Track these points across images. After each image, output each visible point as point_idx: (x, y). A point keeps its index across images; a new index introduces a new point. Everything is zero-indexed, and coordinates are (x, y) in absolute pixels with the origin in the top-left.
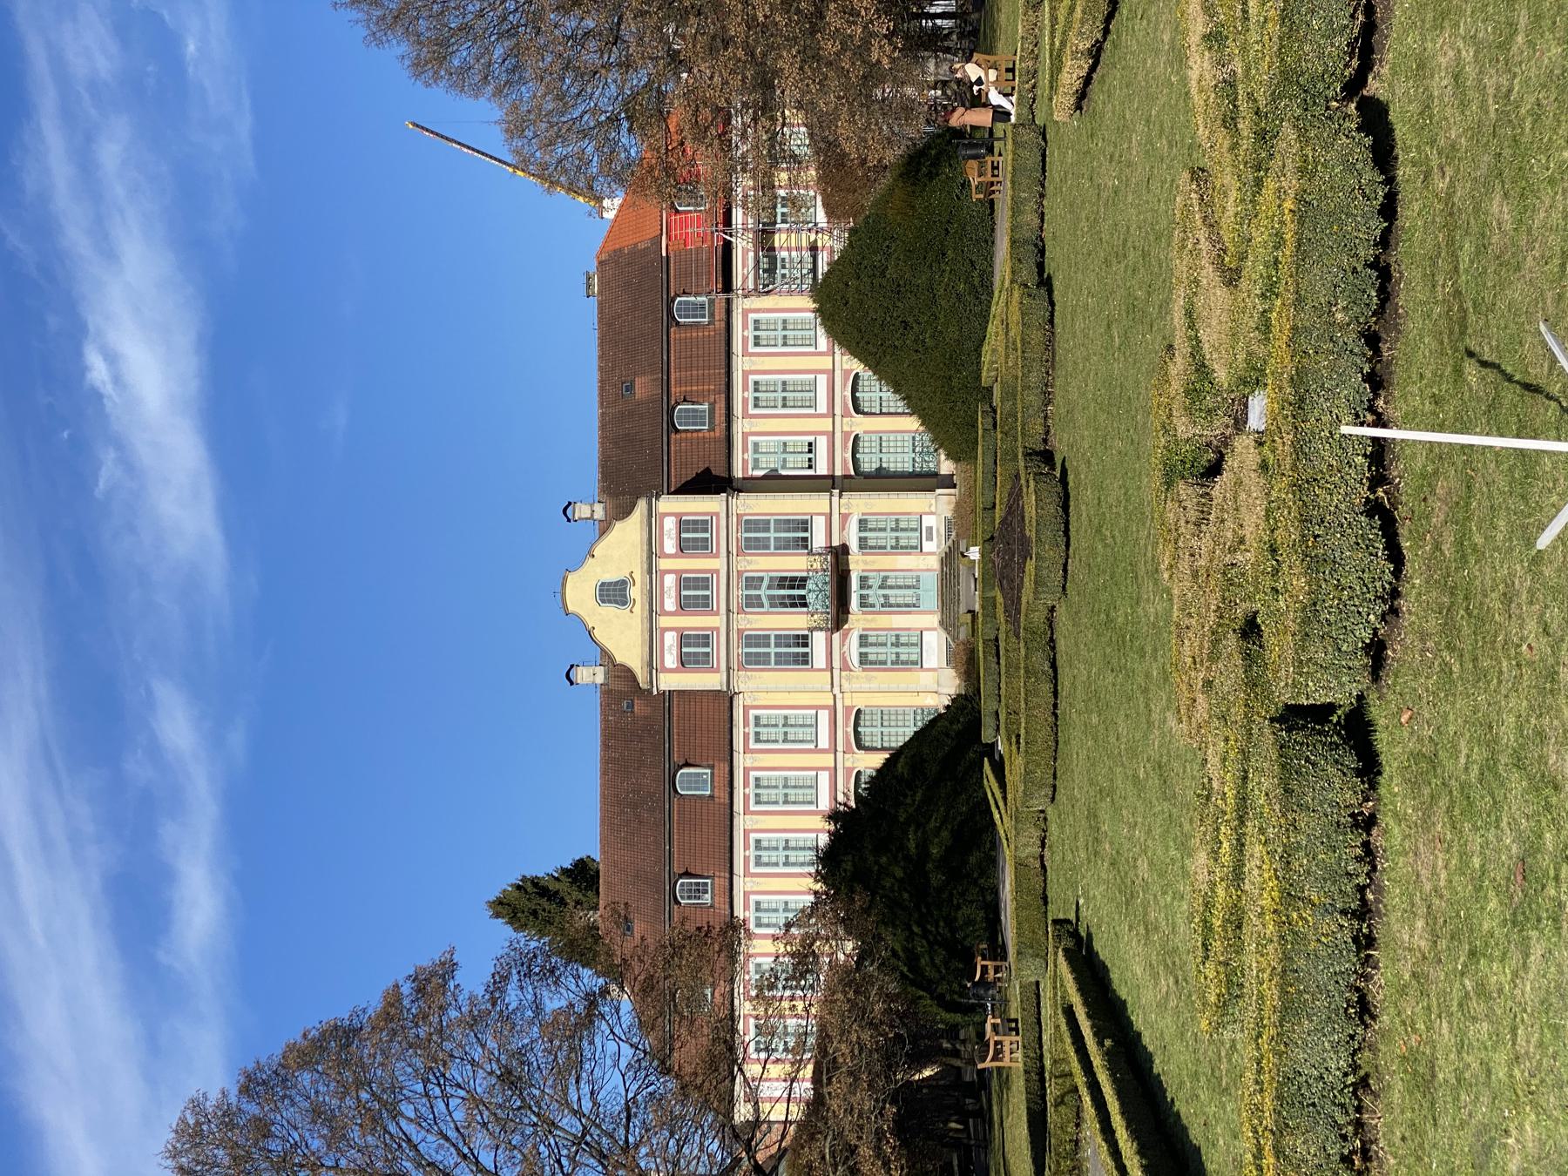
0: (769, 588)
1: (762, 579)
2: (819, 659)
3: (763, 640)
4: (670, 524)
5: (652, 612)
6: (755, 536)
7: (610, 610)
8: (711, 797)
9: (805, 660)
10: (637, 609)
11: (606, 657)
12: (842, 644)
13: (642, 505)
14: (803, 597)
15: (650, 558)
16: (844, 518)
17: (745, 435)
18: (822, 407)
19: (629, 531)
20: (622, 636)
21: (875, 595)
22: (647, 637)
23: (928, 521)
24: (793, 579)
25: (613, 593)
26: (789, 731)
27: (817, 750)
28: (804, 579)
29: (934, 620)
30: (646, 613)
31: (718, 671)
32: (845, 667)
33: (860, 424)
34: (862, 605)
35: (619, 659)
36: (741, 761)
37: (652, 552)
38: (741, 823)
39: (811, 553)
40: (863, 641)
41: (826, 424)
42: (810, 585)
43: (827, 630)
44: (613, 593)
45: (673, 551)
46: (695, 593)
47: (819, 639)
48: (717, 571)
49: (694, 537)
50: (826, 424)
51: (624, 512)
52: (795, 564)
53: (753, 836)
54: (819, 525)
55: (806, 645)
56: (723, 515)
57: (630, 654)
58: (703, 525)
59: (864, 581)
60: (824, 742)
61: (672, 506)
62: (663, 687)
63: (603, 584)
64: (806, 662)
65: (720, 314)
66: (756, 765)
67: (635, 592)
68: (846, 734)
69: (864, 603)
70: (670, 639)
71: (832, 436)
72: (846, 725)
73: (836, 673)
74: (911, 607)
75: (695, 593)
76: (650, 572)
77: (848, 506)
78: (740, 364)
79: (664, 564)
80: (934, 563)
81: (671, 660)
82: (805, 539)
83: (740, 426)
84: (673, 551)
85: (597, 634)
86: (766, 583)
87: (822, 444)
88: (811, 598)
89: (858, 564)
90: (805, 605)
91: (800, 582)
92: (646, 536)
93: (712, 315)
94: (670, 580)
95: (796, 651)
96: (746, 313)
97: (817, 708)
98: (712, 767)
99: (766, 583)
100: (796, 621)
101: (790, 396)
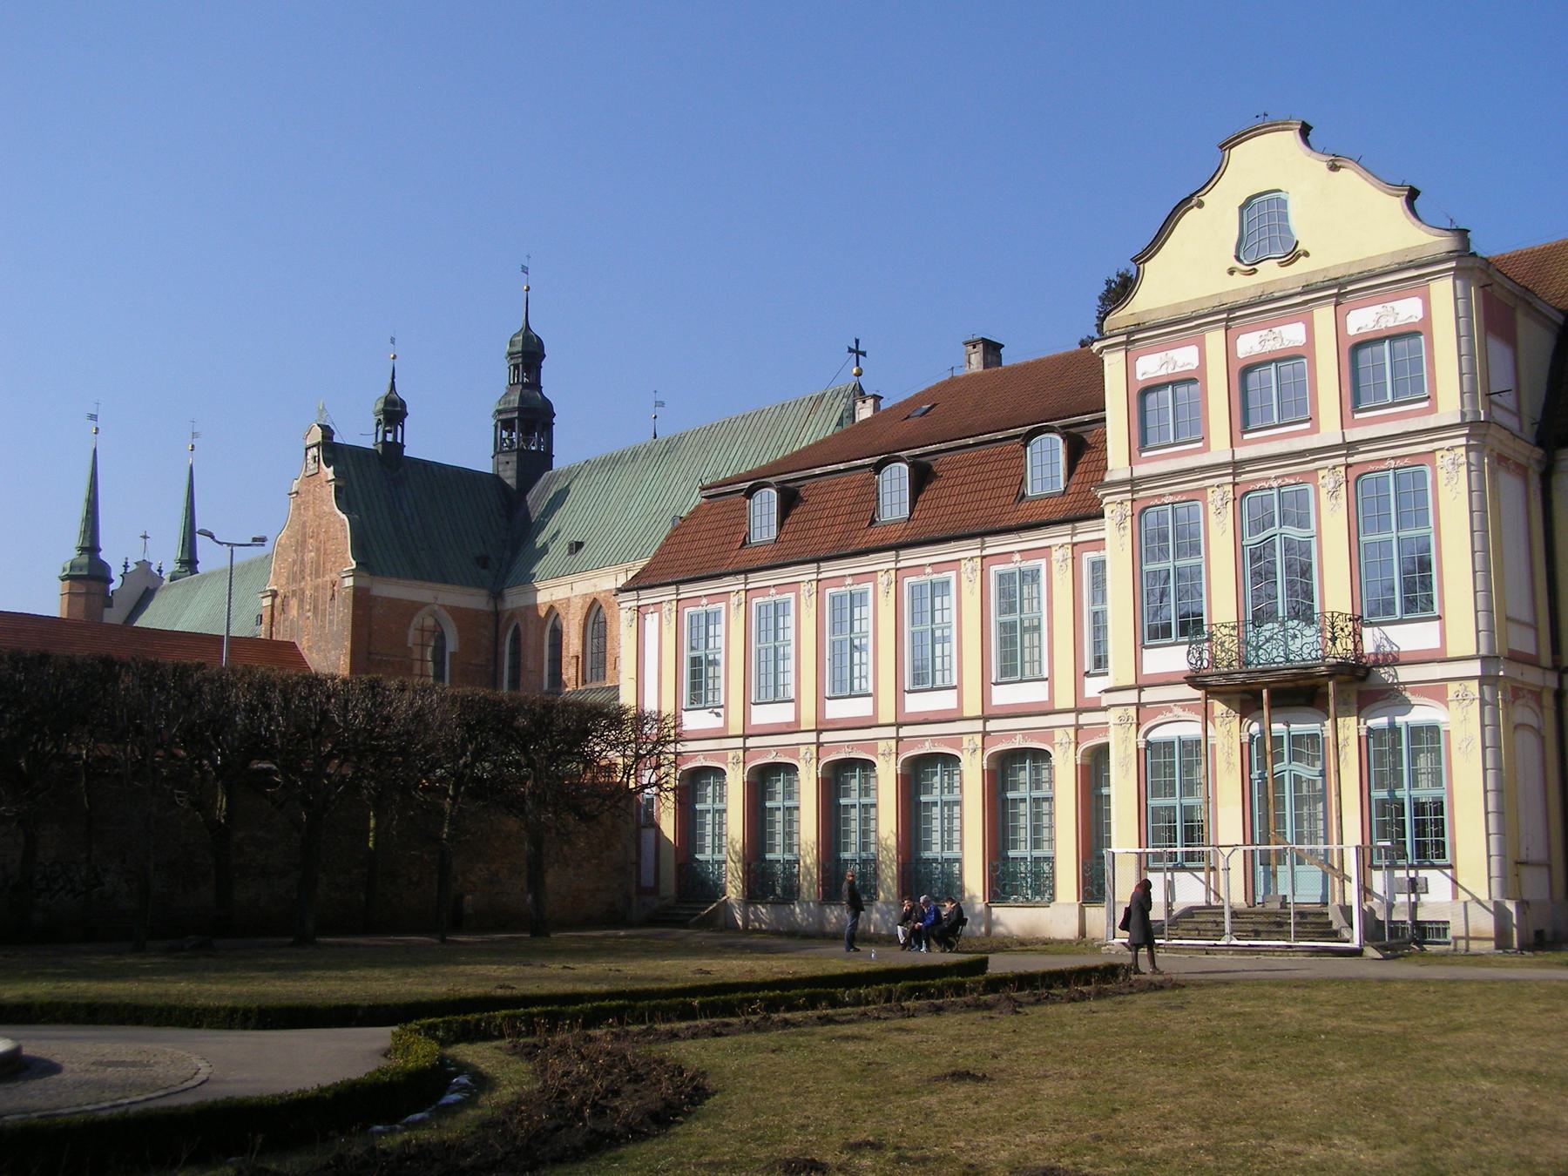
0: (1289, 545)
1: (1302, 523)
4: (1407, 311)
5: (1230, 315)
6: (1387, 497)
8: (1024, 495)
9: (1159, 633)
10: (1240, 281)
14: (1272, 615)
20: (1193, 263)
22: (1187, 312)
23: (1436, 880)
24: (1308, 594)
25: (1263, 227)
27: (1080, 675)
30: (1229, 300)
35: (1150, 267)
38: (967, 551)
40: (1194, 750)
44: (1263, 227)
45: (1352, 329)
47: (1172, 658)
48: (1315, 430)
56: (1432, 421)
58: (1413, 385)
63: (1283, 204)
66: (1055, 566)
67: (1270, 272)
70: (1184, 358)
73: (1132, 696)
75: (1259, 390)
76: (1307, 289)
77: (1462, 698)
79: (1324, 316)
81: (1150, 366)
82: (1388, 607)
84: (1352, 329)
85: (1191, 218)
86: (1294, 532)
89: (1348, 732)
92: (1377, 265)
94: (1292, 335)
99: (1294, 532)
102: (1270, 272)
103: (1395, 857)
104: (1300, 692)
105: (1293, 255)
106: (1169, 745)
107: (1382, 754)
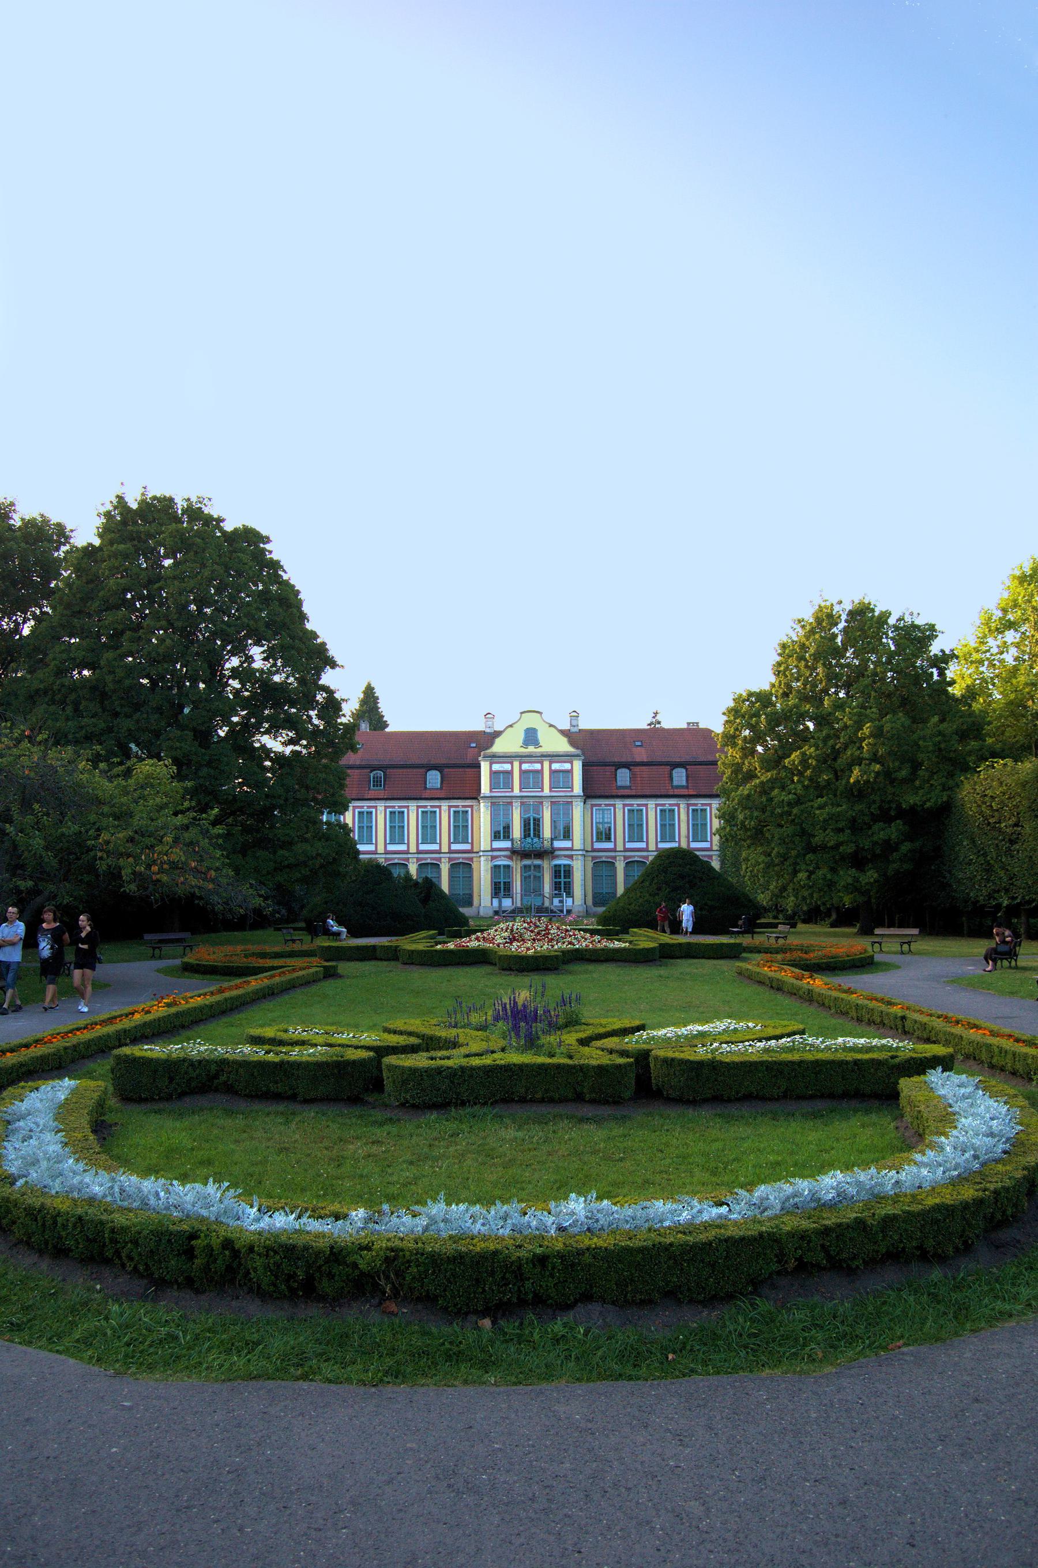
2: (497, 844)
3: (508, 815)
4: (567, 766)
7: (521, 736)
11: (497, 734)
12: (505, 856)
13: (579, 752)
14: (529, 835)
15: (549, 756)
16: (571, 857)
17: (614, 806)
18: (629, 845)
19: (563, 746)
21: (532, 873)
25: (531, 737)
26: (462, 829)
28: (539, 837)
29: (519, 905)
31: (491, 791)
32: (493, 858)
33: (620, 866)
34: (525, 866)
35: (498, 741)
36: (445, 805)
37: (554, 757)
38: (413, 805)
39: (552, 839)
41: (620, 847)
42: (536, 840)
43: (513, 847)
44: (531, 737)
46: (531, 778)
47: (507, 844)
48: (542, 791)
49: (561, 778)
50: (620, 847)
51: (572, 743)
52: (547, 832)
53: (406, 810)
54: (567, 844)
55: (504, 837)
57: (499, 746)
59: (538, 868)
60: (454, 847)
61: (577, 767)
62: (483, 764)
64: (495, 837)
65: (677, 792)
67: (531, 749)
68: (458, 858)
69: (526, 868)
70: (507, 767)
71: (614, 850)
72: (463, 858)
73: (490, 853)
74: (526, 892)
78: (651, 803)
79: (546, 764)
80: (547, 903)
81: (496, 767)
83: (619, 803)
87: (610, 845)
88: (529, 840)
89: (547, 865)
90: (525, 837)
91: (538, 833)
93: (678, 787)
94: (538, 766)
95: (502, 832)
96: (678, 805)
97: (472, 844)
98: (441, 788)
100: (517, 832)
101: (636, 830)
102: (531, 749)
103: (559, 895)
104: (541, 854)
105: (536, 744)
106: (499, 866)
107: (557, 871)
